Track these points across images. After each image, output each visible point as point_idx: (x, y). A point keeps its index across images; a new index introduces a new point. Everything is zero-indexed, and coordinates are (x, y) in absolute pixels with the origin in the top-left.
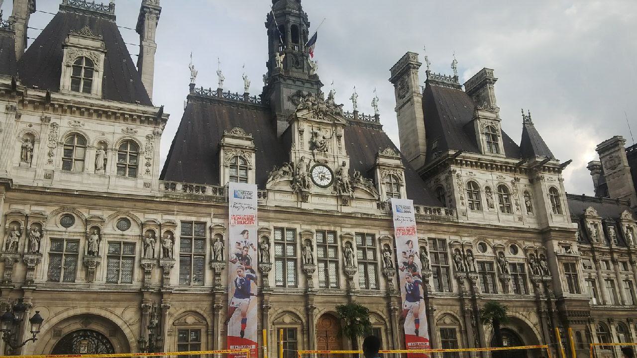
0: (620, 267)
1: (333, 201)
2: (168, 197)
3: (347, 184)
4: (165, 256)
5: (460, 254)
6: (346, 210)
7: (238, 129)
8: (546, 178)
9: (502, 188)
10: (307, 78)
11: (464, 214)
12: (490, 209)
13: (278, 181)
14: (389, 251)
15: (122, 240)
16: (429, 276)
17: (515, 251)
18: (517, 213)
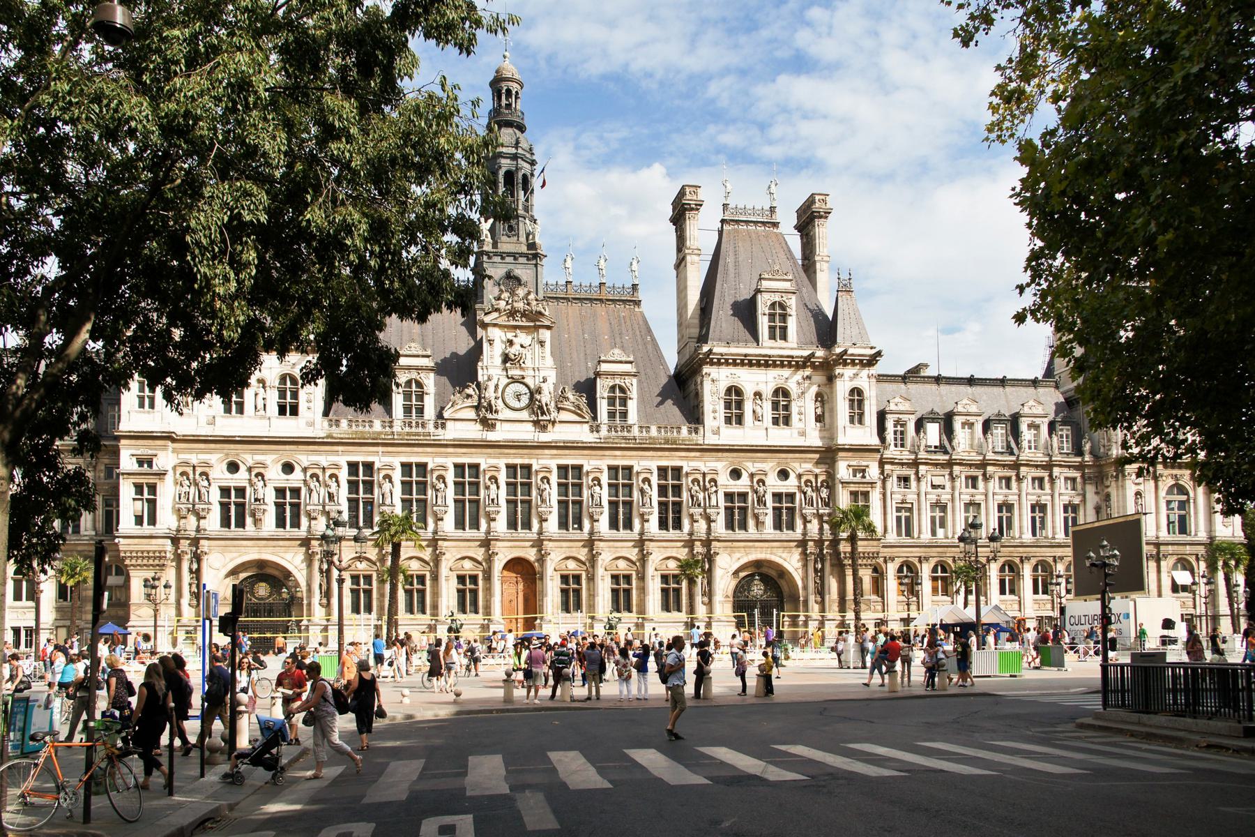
0: (994, 485)
1: (530, 427)
2: (332, 438)
3: (547, 405)
4: (330, 500)
5: (699, 485)
6: (544, 437)
7: (413, 345)
8: (846, 377)
9: (782, 392)
10: (524, 249)
11: (717, 432)
12: (757, 423)
13: (459, 407)
14: (600, 485)
15: (287, 485)
16: (650, 514)
17: (784, 474)
18: (801, 425)
